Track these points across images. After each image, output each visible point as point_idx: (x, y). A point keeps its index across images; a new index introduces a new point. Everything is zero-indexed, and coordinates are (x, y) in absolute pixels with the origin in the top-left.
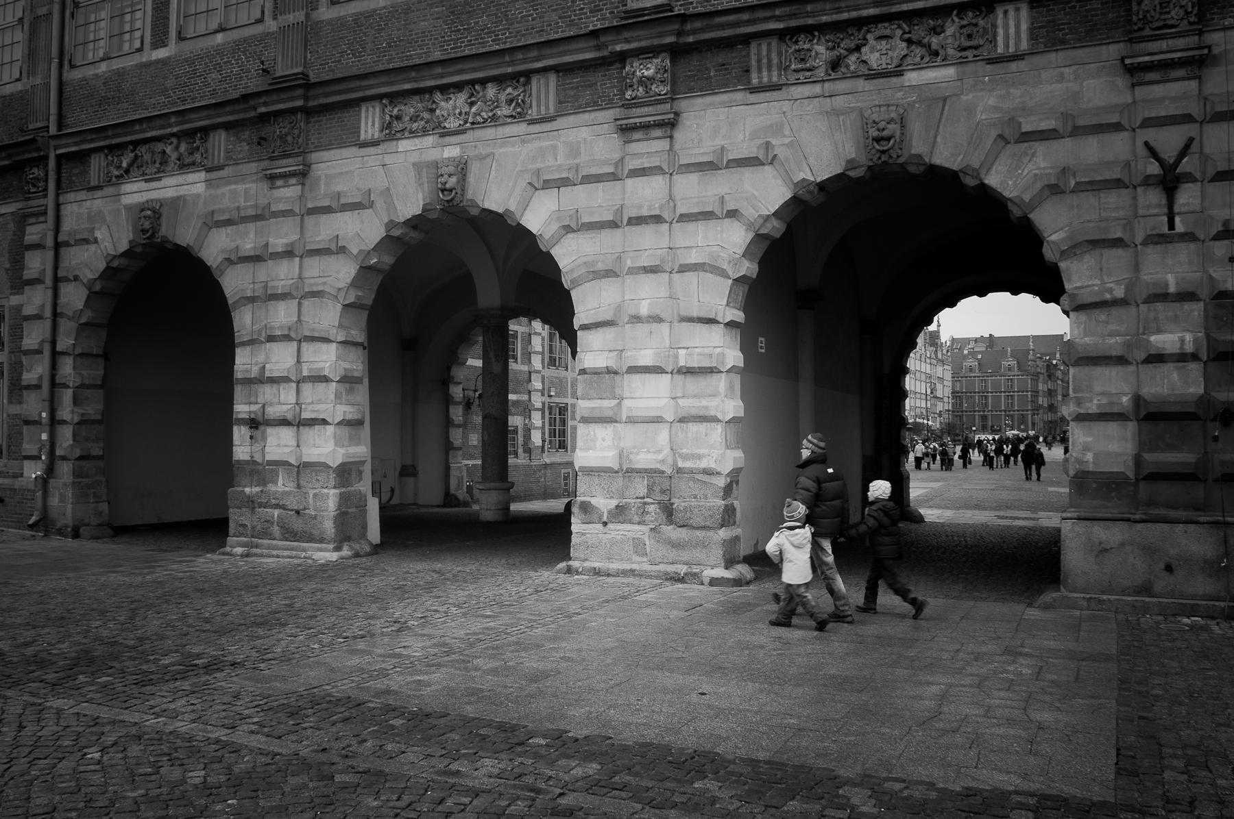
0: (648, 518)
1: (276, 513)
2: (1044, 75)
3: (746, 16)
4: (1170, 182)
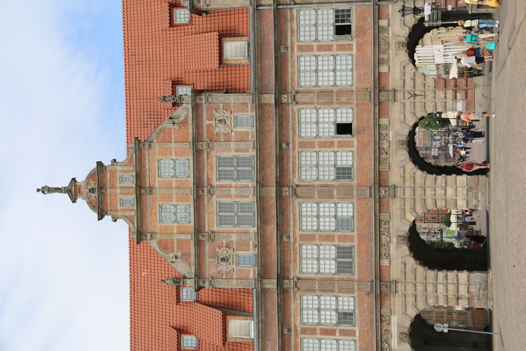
0: (477, 192)
1: (481, 292)
2: (393, 116)
3: (375, 170)
4: (415, 95)
